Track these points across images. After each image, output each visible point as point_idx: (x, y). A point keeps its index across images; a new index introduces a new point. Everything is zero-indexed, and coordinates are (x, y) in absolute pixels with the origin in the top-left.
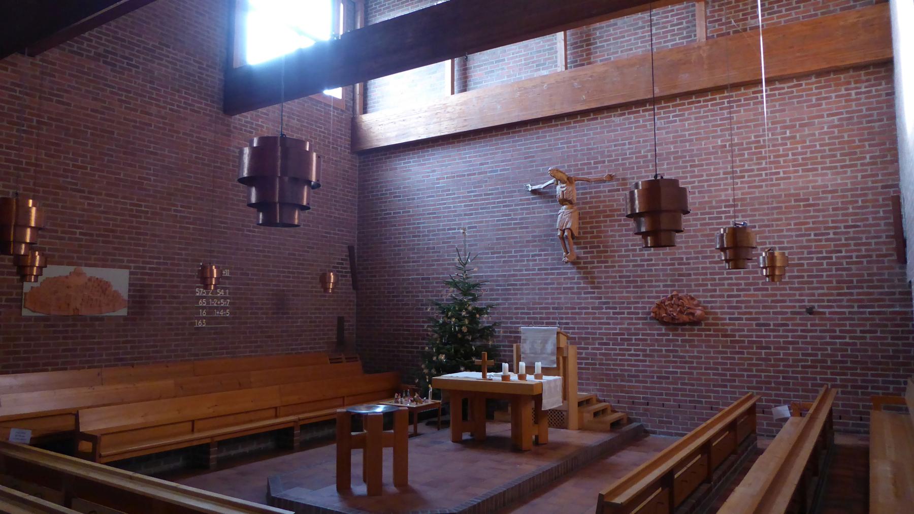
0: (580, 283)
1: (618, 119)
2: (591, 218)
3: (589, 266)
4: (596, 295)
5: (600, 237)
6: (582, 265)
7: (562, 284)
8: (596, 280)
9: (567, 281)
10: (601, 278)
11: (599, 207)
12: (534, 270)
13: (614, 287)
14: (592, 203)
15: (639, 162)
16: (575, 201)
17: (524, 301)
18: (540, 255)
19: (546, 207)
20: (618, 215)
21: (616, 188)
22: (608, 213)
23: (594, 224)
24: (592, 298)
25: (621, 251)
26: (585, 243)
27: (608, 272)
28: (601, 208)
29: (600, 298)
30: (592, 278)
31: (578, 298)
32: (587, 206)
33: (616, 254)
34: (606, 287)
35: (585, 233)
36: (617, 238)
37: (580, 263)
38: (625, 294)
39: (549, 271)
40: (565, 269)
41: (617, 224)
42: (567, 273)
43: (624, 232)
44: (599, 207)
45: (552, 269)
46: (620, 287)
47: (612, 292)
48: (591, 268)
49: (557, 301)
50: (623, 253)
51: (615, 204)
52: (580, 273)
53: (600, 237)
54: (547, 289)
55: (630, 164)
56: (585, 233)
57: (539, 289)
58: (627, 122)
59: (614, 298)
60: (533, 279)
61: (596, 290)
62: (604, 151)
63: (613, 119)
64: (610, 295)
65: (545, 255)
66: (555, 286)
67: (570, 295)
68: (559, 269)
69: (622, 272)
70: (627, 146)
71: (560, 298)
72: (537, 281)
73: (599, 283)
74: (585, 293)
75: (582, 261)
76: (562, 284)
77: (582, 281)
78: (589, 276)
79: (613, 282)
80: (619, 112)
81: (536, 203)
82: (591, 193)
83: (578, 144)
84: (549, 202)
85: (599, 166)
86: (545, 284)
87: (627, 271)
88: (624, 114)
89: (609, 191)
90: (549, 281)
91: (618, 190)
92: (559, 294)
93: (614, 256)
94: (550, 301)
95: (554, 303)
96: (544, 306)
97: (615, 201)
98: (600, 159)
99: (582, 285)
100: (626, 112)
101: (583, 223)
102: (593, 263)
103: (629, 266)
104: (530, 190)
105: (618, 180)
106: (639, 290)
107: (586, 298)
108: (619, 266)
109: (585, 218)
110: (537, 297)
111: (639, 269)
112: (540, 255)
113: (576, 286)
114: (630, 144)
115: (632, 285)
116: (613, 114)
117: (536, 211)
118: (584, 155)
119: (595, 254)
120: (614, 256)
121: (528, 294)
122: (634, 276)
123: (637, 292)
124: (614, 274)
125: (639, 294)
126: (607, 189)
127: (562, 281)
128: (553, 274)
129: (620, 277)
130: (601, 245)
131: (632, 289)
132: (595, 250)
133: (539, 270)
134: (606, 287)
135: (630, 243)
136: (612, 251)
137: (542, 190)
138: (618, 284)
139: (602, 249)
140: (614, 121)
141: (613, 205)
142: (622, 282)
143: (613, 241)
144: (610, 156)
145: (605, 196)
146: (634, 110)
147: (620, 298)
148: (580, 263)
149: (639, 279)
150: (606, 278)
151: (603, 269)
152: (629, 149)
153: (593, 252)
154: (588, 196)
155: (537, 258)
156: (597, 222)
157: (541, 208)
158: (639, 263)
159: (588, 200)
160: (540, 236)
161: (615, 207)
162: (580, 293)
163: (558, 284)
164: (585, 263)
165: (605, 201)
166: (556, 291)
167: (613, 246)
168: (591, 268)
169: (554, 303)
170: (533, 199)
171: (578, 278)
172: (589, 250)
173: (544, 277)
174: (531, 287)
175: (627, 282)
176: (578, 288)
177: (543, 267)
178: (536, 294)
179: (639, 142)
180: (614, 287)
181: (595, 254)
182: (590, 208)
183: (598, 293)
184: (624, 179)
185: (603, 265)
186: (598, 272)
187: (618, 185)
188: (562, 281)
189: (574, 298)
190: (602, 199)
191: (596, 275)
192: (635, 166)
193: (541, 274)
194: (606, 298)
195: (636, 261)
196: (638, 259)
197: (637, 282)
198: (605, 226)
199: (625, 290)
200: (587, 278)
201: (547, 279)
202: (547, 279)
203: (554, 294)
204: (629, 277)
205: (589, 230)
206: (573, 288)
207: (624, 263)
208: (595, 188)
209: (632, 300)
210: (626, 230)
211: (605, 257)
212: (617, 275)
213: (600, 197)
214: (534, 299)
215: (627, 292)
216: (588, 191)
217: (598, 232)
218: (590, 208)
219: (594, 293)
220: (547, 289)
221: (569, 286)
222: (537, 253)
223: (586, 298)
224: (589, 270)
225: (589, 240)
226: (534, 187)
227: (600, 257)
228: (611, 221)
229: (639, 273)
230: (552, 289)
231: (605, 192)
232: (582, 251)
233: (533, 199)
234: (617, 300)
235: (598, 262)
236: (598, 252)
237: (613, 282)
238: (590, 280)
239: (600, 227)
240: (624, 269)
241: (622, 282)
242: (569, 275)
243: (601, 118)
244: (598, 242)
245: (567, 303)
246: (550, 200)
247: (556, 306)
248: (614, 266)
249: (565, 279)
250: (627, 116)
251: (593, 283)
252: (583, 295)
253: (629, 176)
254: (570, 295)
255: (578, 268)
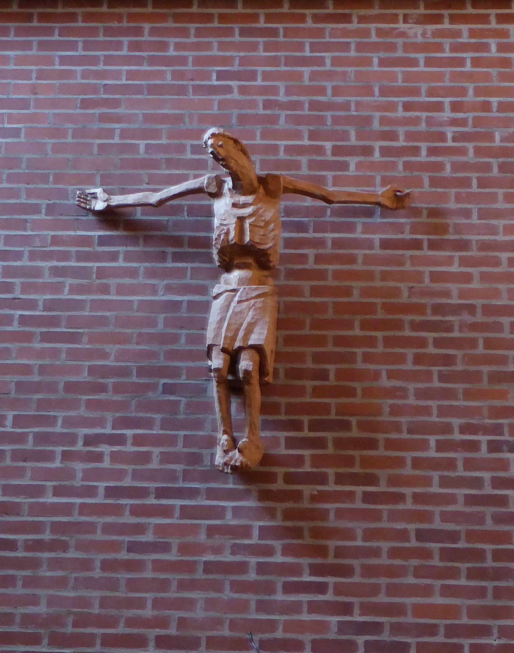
0: (269, 551)
1: (419, 29)
2: (317, 325)
3: (307, 490)
4: (329, 597)
5: (351, 393)
6: (280, 485)
7: (198, 549)
8: (332, 544)
9: (218, 540)
10: (348, 535)
11: (348, 292)
12: (91, 491)
13: (401, 572)
14: (321, 275)
15: (487, 167)
16: (274, 260)
17: (42, 609)
18: (119, 440)
19: (151, 273)
20: (416, 326)
21: (407, 236)
22: (380, 315)
23: (330, 348)
24: (313, 607)
25: (423, 445)
26: (291, 409)
27: (376, 516)
28: (356, 297)
29: (347, 609)
30: (316, 533)
31: (262, 606)
32: (306, 285)
33: (409, 455)
34: (368, 571)
35: (292, 374)
36: (412, 401)
37: (271, 478)
38: (438, 600)
39: (152, 501)
40: (212, 494)
41: (410, 353)
42: (219, 513)
43: (436, 384)
44: (348, 292)
45: (161, 493)
46: (418, 572)
47: (392, 590)
48: (314, 498)
49: (177, 614)
50: (432, 453)
51: (403, 286)
52: (271, 513)
53: (351, 393)
54: (137, 566)
55: (456, 167)
56: (292, 374)
57: (106, 565)
58: (447, 42)
59: (400, 610)
60: (79, 527)
61: (330, 580)
62: (368, 120)
63: (401, 26)
64: (382, 598)
65: (138, 440)
66: (172, 556)
67: (228, 594)
68: (192, 493)
69: (424, 517)
70: (447, 114)
71: (189, 604)
72: (99, 536)
73: (340, 552)
74: (289, 588)
75: (280, 471)
76: (198, 549)
77: (277, 544)
78: (305, 524)
79: (394, 553)
80: (422, 10)
81: (114, 257)
82: (320, 243)
83: (281, 85)
84: (162, 257)
85: (353, 161)
86: (132, 547)
87: (446, 517)
88: (438, 19)
89: (385, 244)
90: (148, 537)
91: (416, 245)
92: (183, 586)
93: (399, 462)
94: (148, 612)
95: (163, 623)
96: (121, 629)
97: (403, 276)
98: (353, 141)
99: (278, 558)
100: (446, 12)
101: (288, 340)
102: (322, 479)
103: (451, 499)
104: (99, 205)
105: (416, 212)
106: (489, 585)
107: (295, 608)
108: (417, 498)
109: (300, 324)
110: (96, 594)
111: (489, 510)
112: (119, 440)
113: (253, 560)
114: (455, 107)
115: (464, 566)
116: (401, 12)
117: (113, 282)
118: (298, 120)
119: (330, 450)
120: (399, 462)
121: (61, 583)
122: (471, 536)
123: (481, 593)
124: (399, 526)
125: (489, 601)
126: (377, 237)
127: (202, 537)
128: (166, 512)
129: (421, 535)
130: (354, 420)
131: (463, 582)
132: (329, 435)
133: (111, 492)
134: (368, 571)
135: (456, 422)
136: (391, 444)
137: (139, 215)
138: (415, 562)
139: (355, 433)
140: (403, 34)
141: (396, 292)
142: (426, 554)
143: (395, 411)
144: (392, 136)
145: (367, 260)
146: (470, 10)
147: (419, 610)
148: (271, 478)
149: (488, 547)
150: (369, 535)
151: (359, 505)
152: (454, 122)
153: (320, 443)
154: (310, 252)
155: (105, 449)
156: (340, 341)
157: (133, 273)
158: (488, 490)
159: (310, 265)
160: (123, 372)
161: (404, 298)
162: (269, 588)
163: (184, 549)
164: (289, 478)
165: (369, 276)
166: (174, 577)
167: (397, 427)
168: (315, 498)
169: (163, 623)
170: (102, 241)
171: (264, 532)
172: (306, 433)
173: (127, 519)
174: (72, 554)
175: (446, 554)
176: (262, 568)
177: (127, 482)
178: (91, 583)
179: (486, 106)
180: (401, 572)
181: (330, 450)
182: (315, 291)
183: (339, 590)
184: (434, 213)
185: (359, 490)
186: (340, 514)
187: (414, 229)
188: (202, 537)
189: (243, 606)
190: (358, 267)
191: (332, 522)
192: (474, 176)
193: (117, 510)
194: (366, 609)
195: (477, 483)
196: (487, 475)
197: (479, 555)
198: (367, 358)
199: (438, 583)
200: (297, 533)
201: (140, 529)
202: (140, 529)
203: (164, 585)
204: (453, 536)
205: (309, 364)
206: (242, 567)
207: (435, 489)
208: (336, 228)
209: (465, 620)
210: (443, 378)
211: (365, 463)
212: (412, 527)
213: (351, 260)
214: (84, 602)
215: (447, 591)
216: (310, 235)
217: (341, 375)
218: (315, 291)
219: (321, 588)
220: (137, 566)
221: (227, 557)
222: (108, 430)
223: (295, 608)
224: (306, 504)
225: (308, 399)
226: (117, 200)
227: (349, 461)
228: (388, 341)
229: (489, 525)
230: (159, 566)
231: (369, 244)
232: (282, 435)
233: (102, 241)
234: (409, 619)
235: (340, 479)
236: (339, 443)
237: (394, 553)
238: (308, 540)
239: (351, 358)
240: (437, 510)
241: (426, 554)
242: (230, 520)
243: (362, 19)
244: (342, 410)
245: (217, 623)
246: (170, 250)
247: (172, 631)
248: (399, 498)
249: (212, 531)
250: (446, 25)
251: (322, 551)
252: (280, 597)
253: (452, 205)
254: (228, 594)
255: (264, 495)
